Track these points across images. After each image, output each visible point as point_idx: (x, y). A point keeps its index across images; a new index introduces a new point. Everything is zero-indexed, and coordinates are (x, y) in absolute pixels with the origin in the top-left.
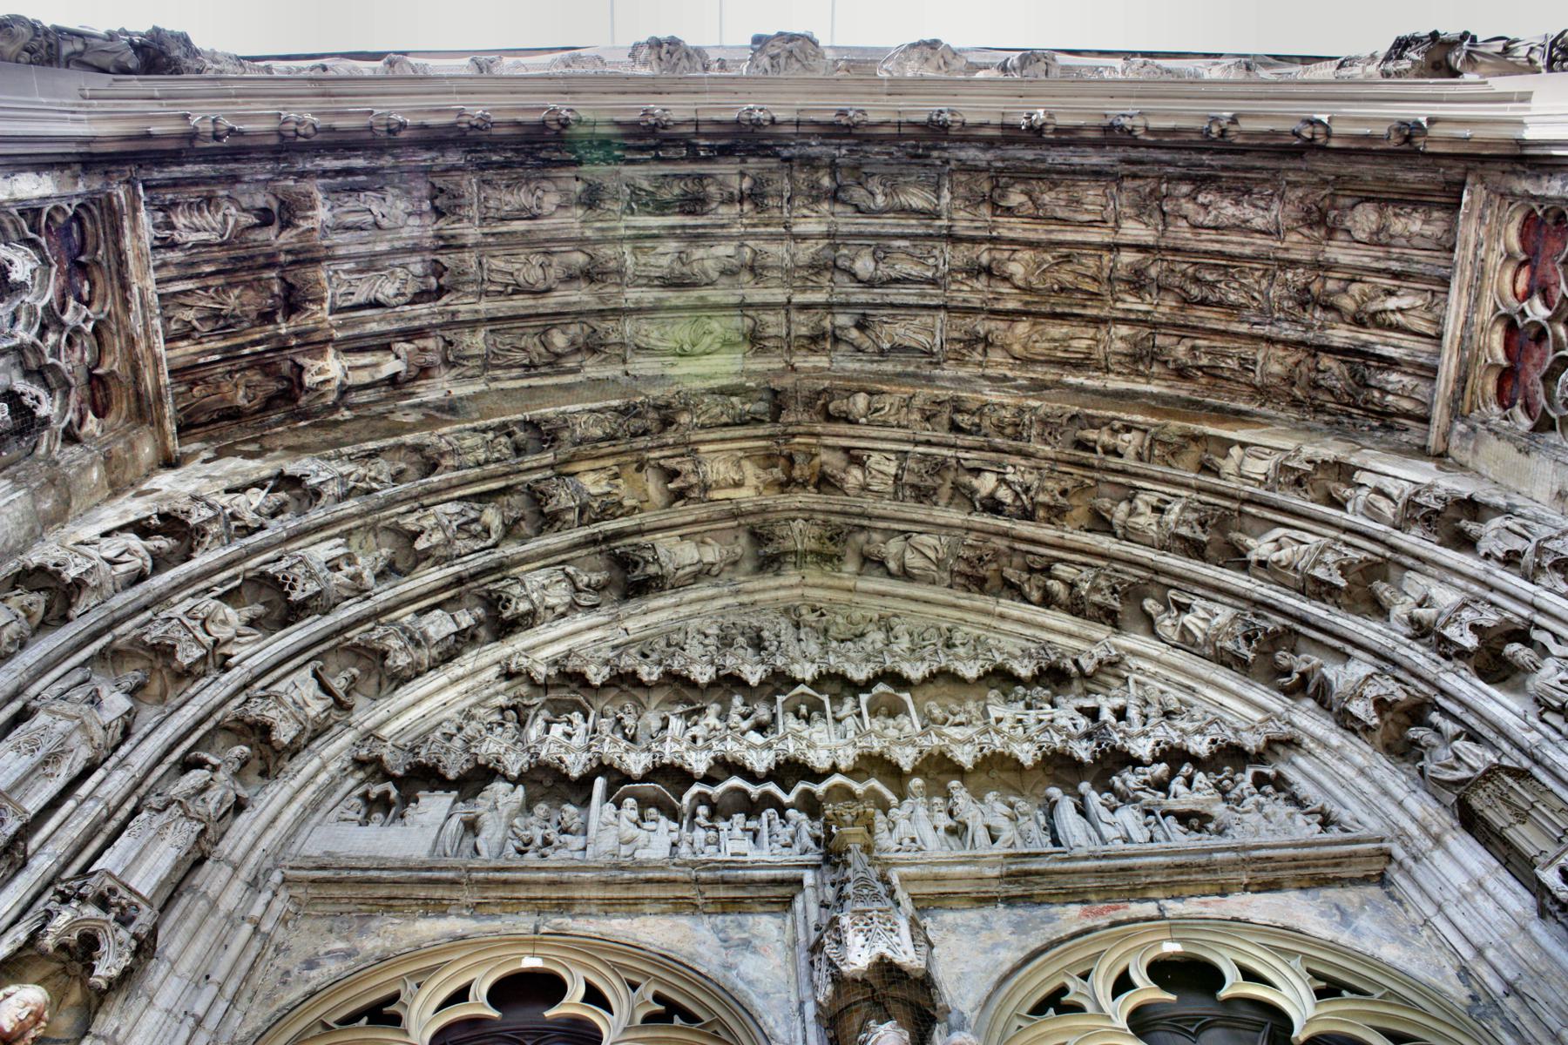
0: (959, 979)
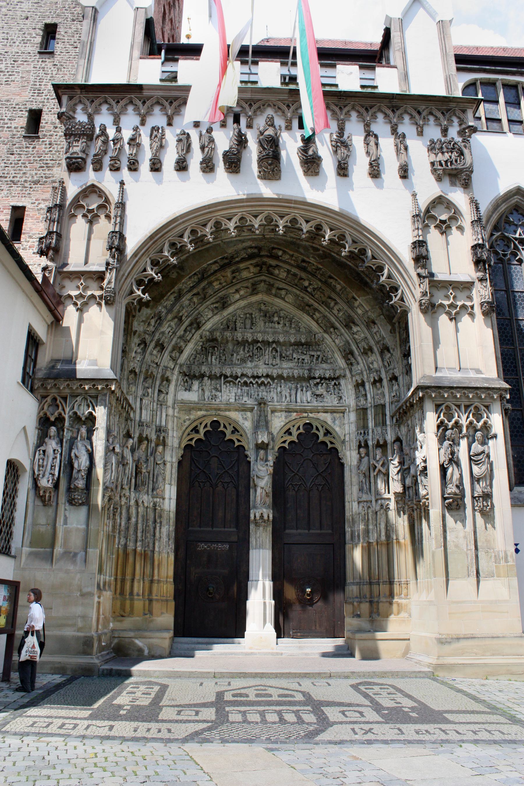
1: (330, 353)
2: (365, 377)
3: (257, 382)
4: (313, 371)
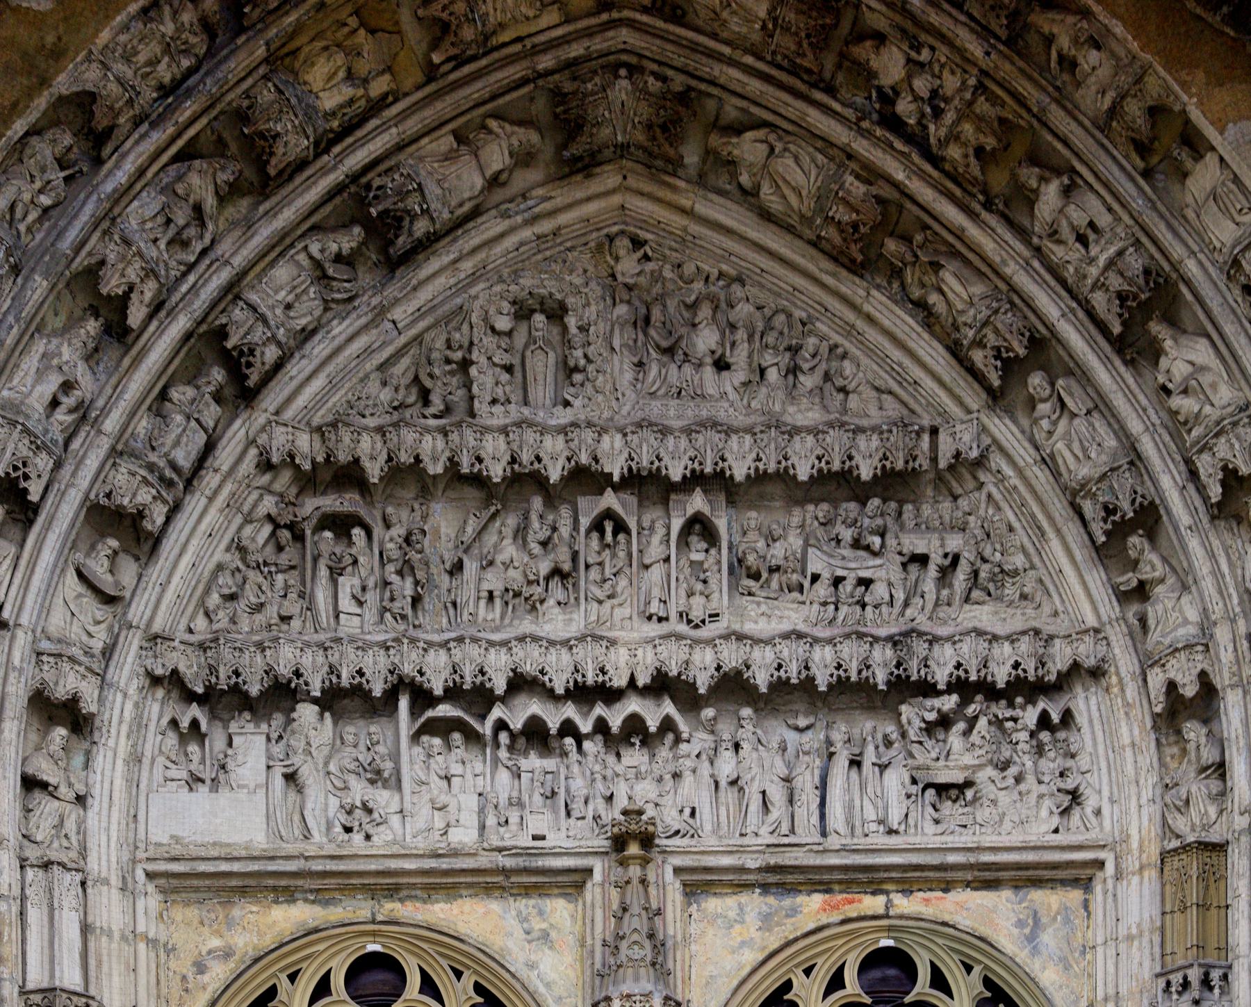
1: (1021, 537)
2: (1226, 656)
3: (601, 727)
4: (920, 647)
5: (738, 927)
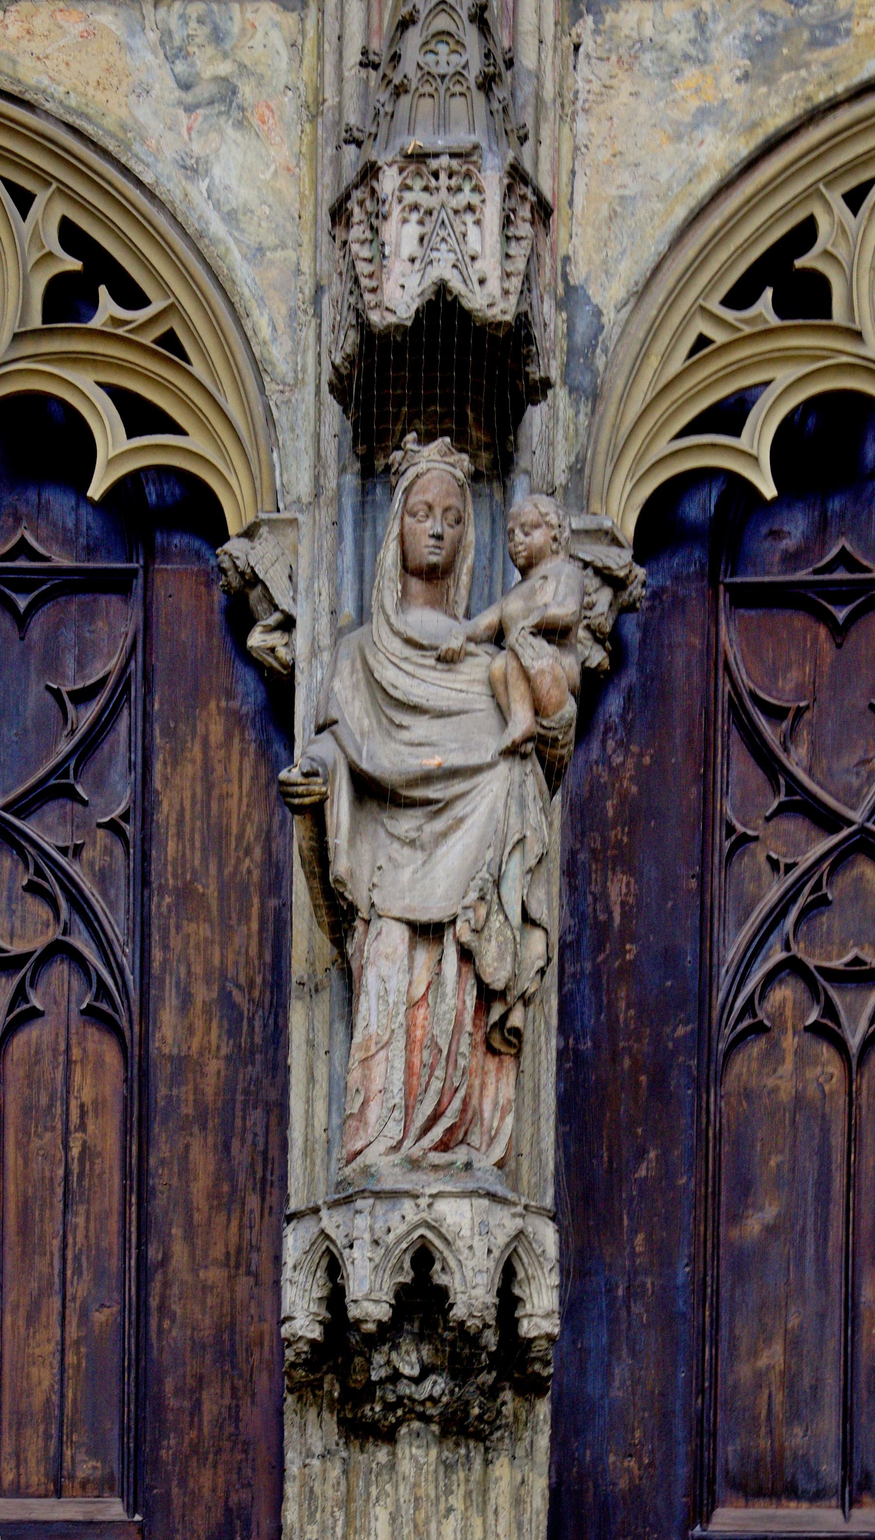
0: (613, 216)
5: (691, 72)
